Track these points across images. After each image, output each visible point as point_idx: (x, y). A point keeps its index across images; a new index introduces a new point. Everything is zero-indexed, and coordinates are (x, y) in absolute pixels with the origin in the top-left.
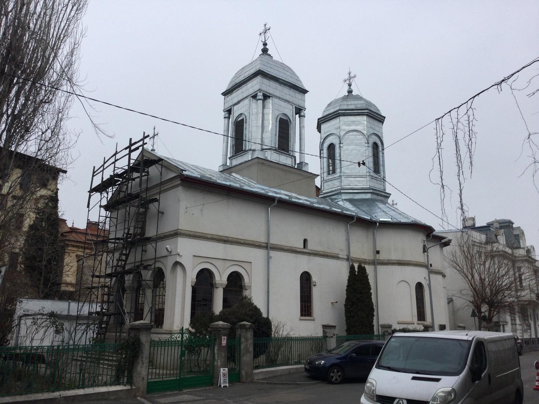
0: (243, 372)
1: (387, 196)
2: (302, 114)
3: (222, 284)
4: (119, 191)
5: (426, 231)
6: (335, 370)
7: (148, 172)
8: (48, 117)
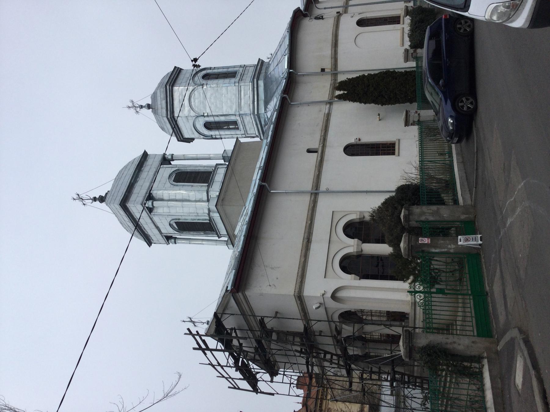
0: (463, 217)
1: (261, 63)
2: (170, 157)
3: (358, 245)
5: (298, 17)
6: (460, 104)
7: (232, 329)
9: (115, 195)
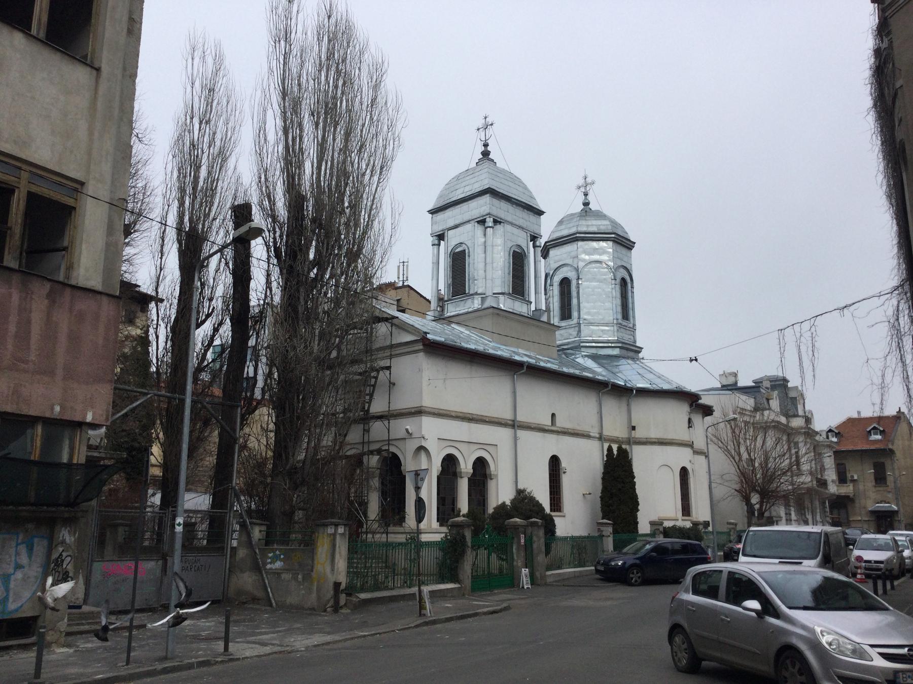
1: (638, 350)
5: (691, 399)
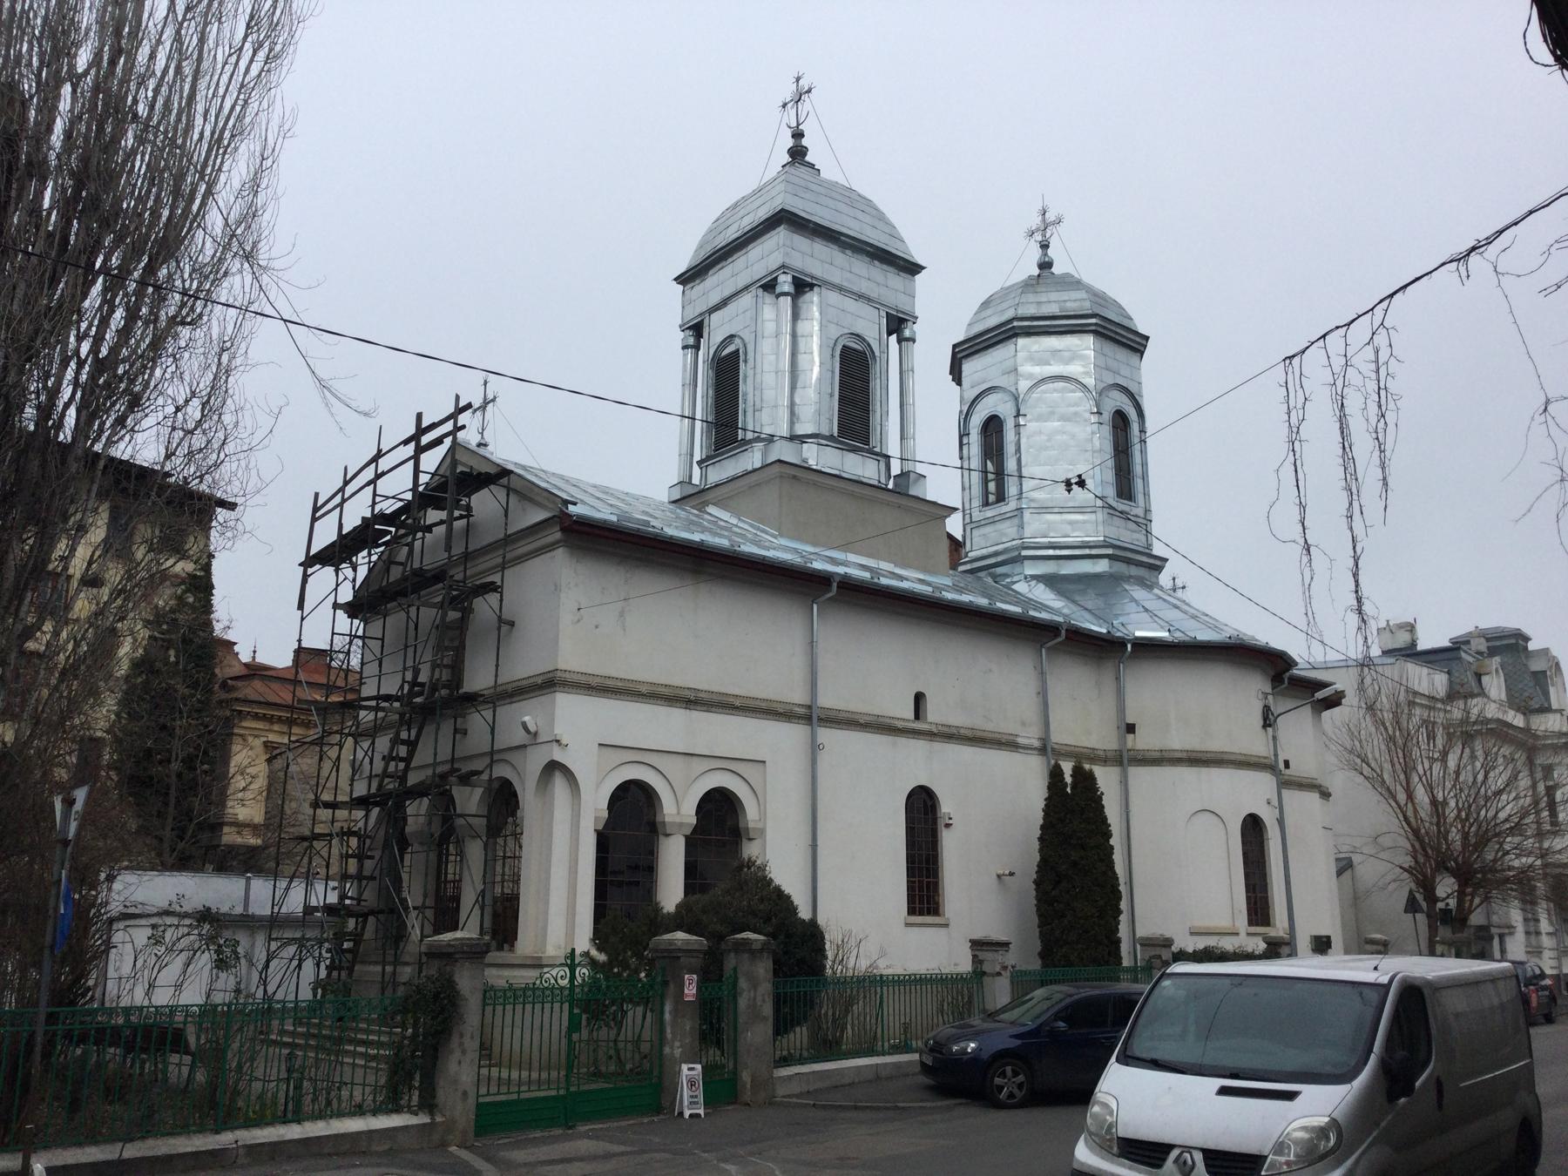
0: (746, 1076)
1: (1157, 565)
3: (681, 825)
4: (387, 563)
5: (1273, 665)
6: (1009, 1069)
7: (468, 508)
8: (191, 363)
9: (807, 196)
